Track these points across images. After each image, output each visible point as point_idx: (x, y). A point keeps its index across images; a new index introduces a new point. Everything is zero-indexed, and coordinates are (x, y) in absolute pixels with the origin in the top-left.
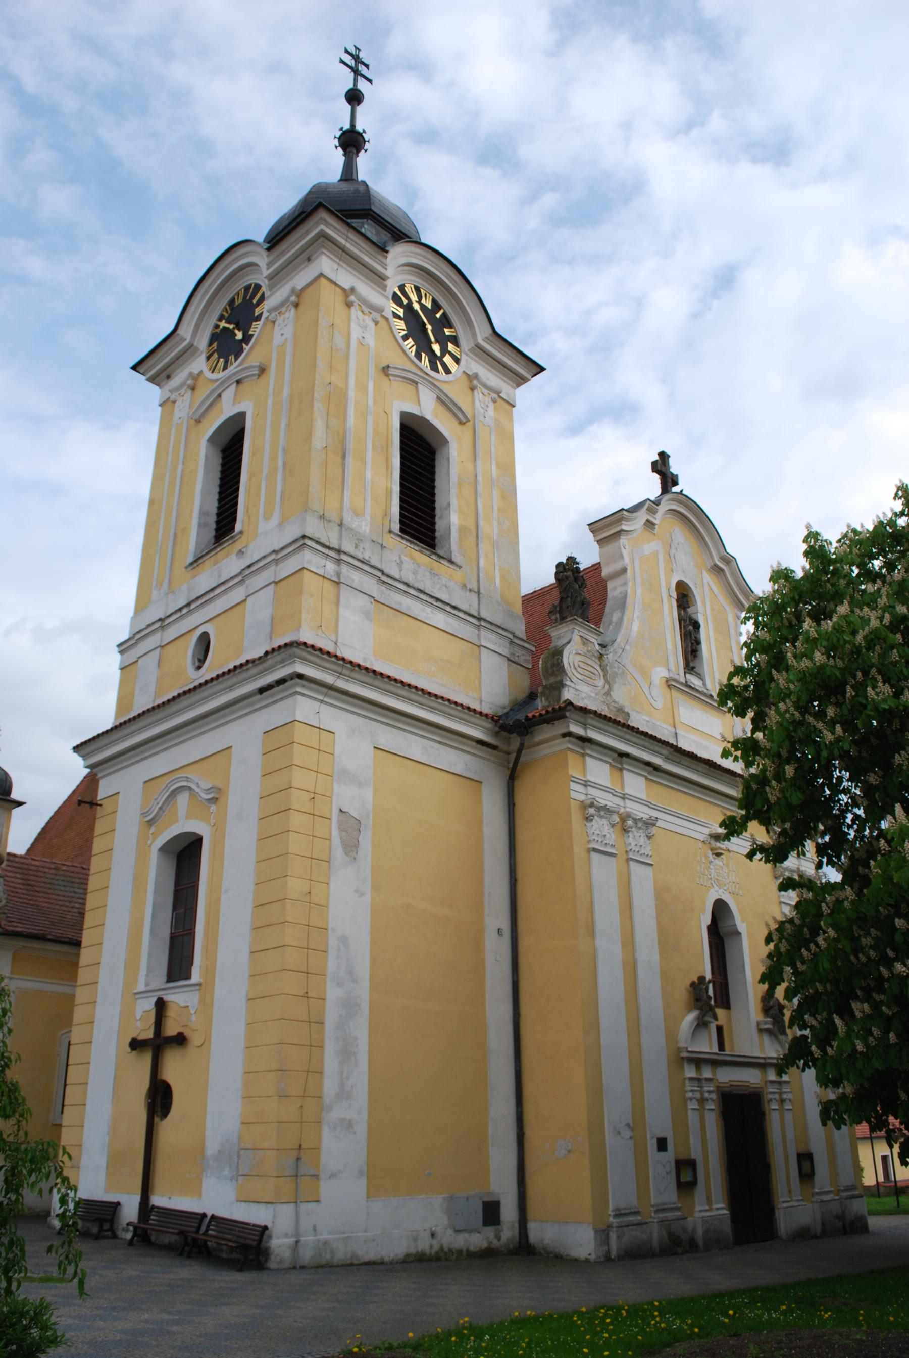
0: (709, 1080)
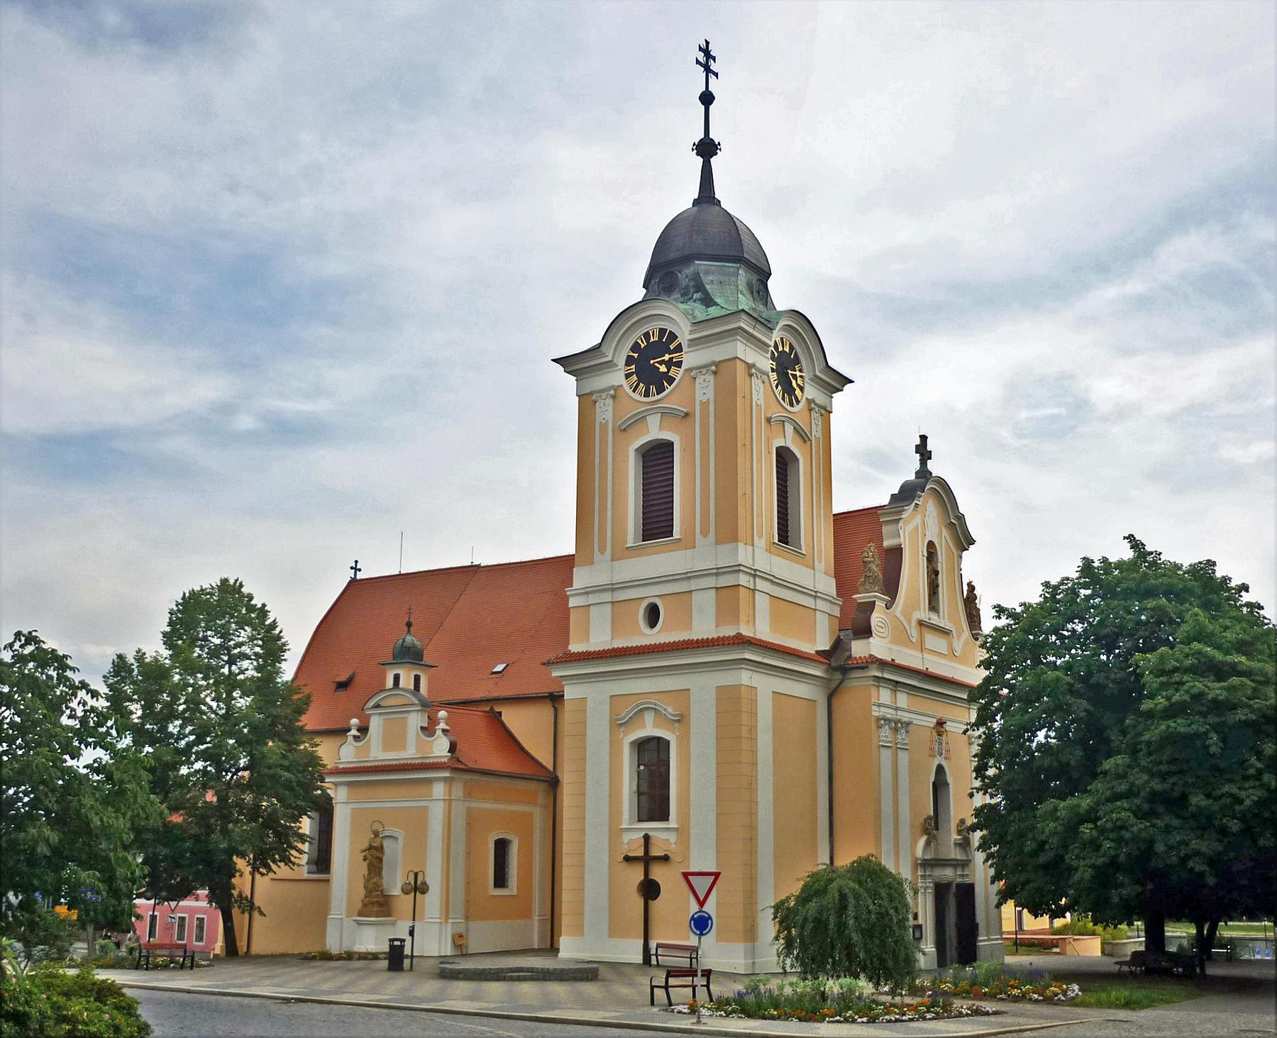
0: (929, 876)
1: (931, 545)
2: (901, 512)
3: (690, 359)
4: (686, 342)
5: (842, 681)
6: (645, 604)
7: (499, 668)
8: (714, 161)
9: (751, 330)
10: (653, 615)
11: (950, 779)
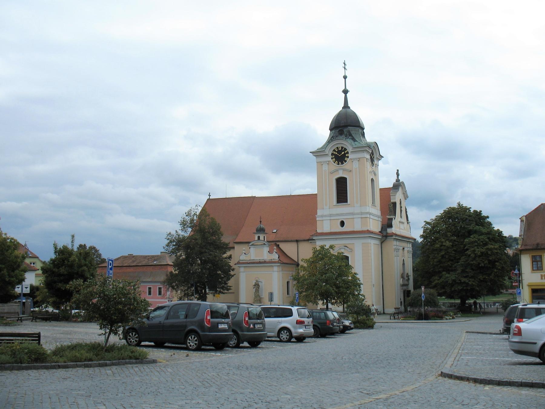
1: (400, 199)
2: (396, 193)
3: (351, 156)
4: (350, 152)
5: (386, 239)
6: (340, 220)
7: (275, 231)
8: (347, 95)
9: (368, 150)
10: (342, 224)
11: (405, 263)
